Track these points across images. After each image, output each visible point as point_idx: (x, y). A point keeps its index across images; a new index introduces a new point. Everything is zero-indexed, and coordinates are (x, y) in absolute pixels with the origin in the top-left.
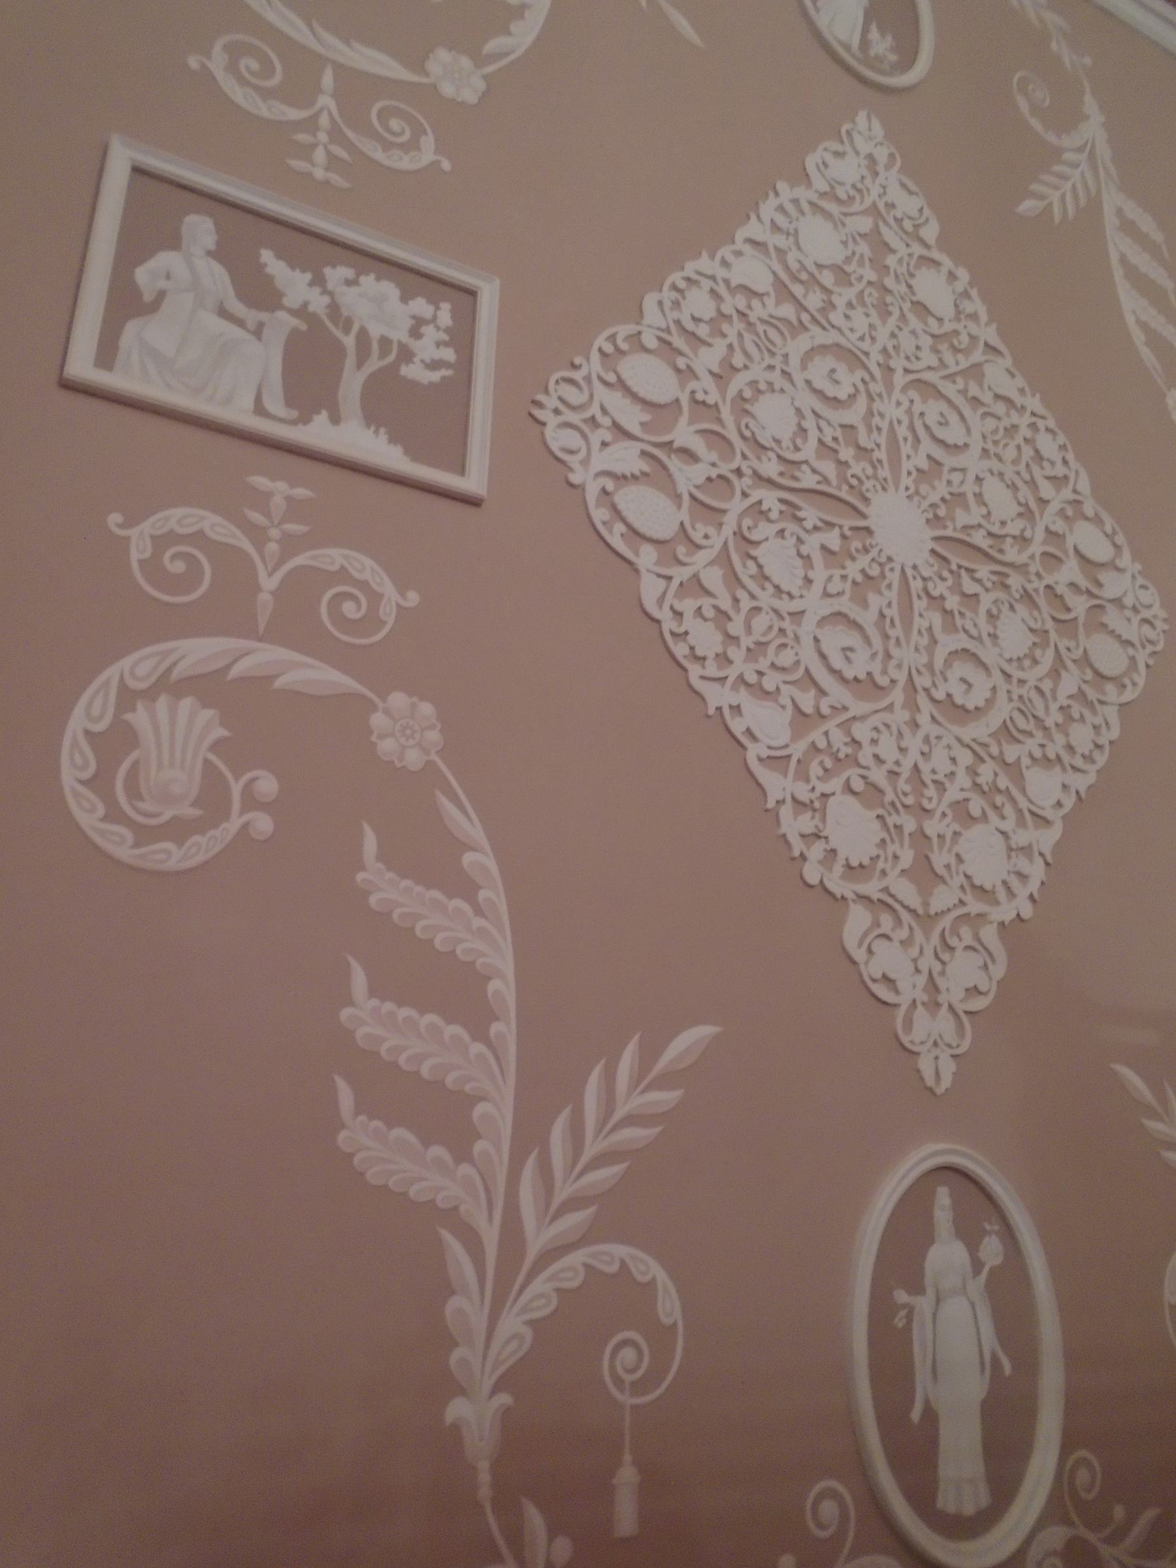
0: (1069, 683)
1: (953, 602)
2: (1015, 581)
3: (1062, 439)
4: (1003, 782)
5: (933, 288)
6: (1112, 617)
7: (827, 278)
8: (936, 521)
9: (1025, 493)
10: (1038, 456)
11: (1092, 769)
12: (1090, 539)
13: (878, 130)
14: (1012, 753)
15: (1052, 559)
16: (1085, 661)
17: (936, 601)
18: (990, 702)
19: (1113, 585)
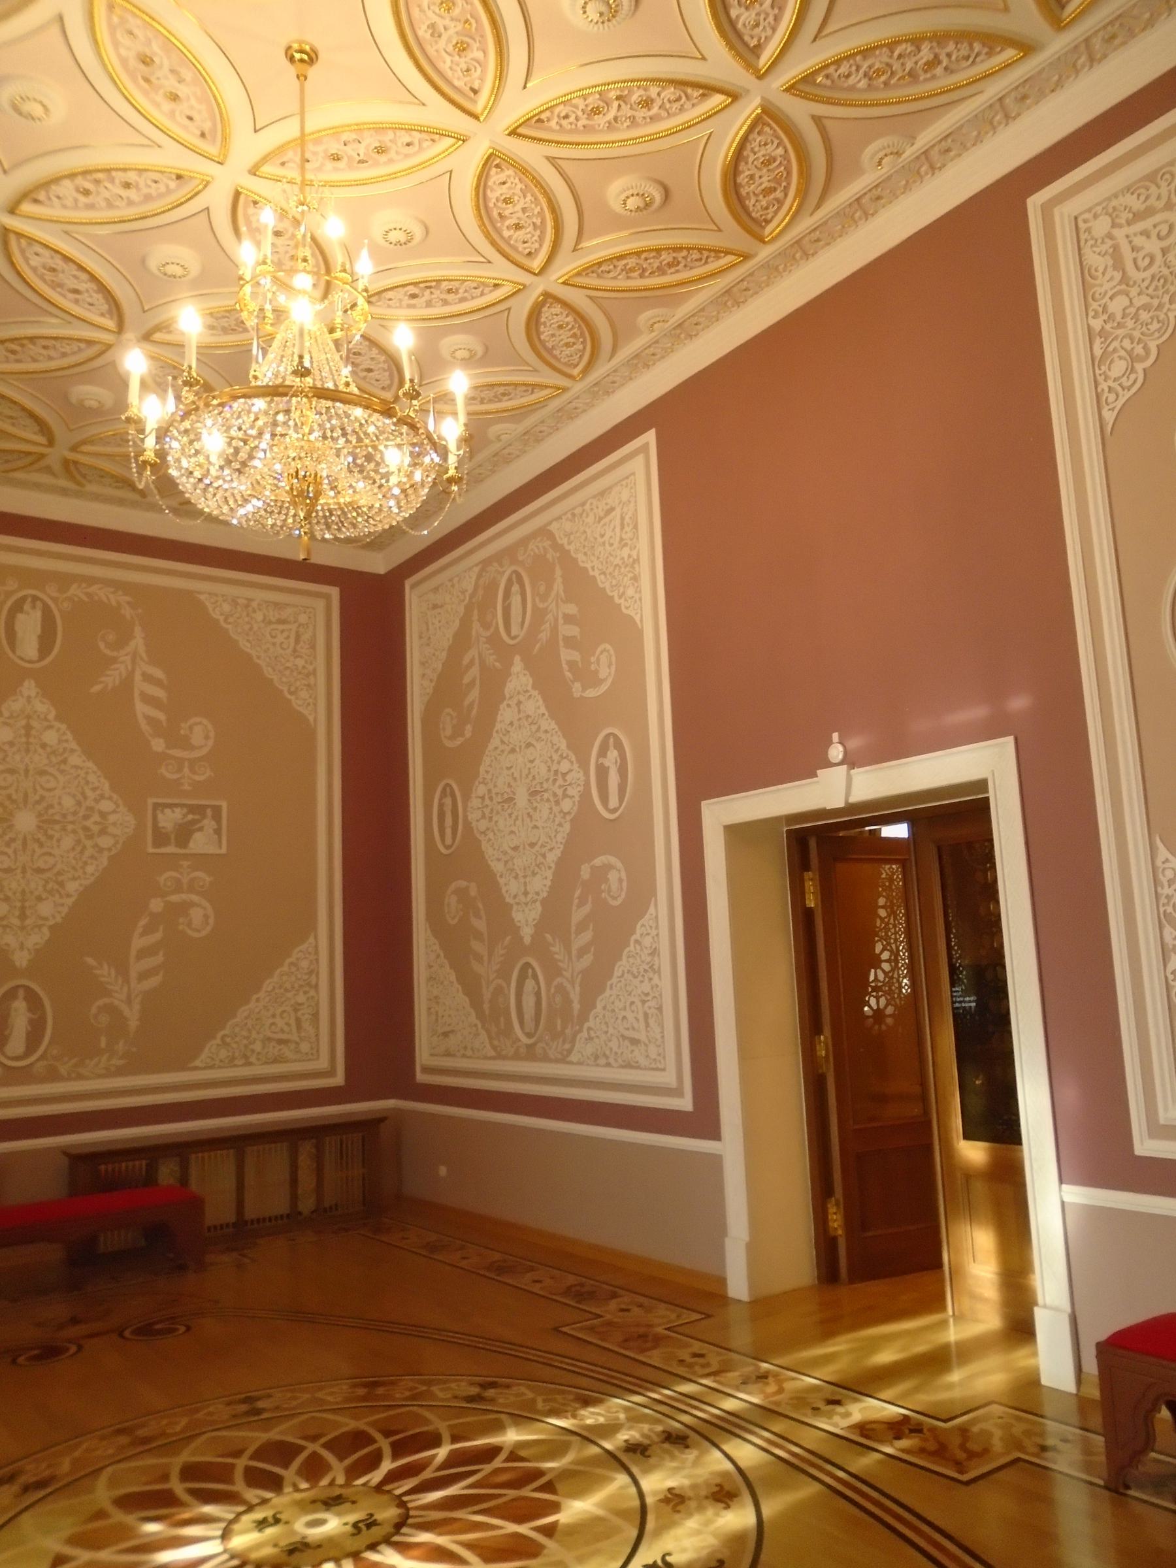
0: (87, 853)
1: (43, 839)
2: (70, 827)
3: (99, 773)
4: (56, 887)
5: (50, 737)
6: (111, 830)
7: (6, 747)
8: (40, 815)
9: (80, 797)
10: (87, 783)
11: (92, 879)
12: (106, 806)
13: (33, 683)
14: (60, 878)
15: (86, 817)
16: (96, 845)
17: (38, 841)
18: (55, 865)
19: (112, 818)
